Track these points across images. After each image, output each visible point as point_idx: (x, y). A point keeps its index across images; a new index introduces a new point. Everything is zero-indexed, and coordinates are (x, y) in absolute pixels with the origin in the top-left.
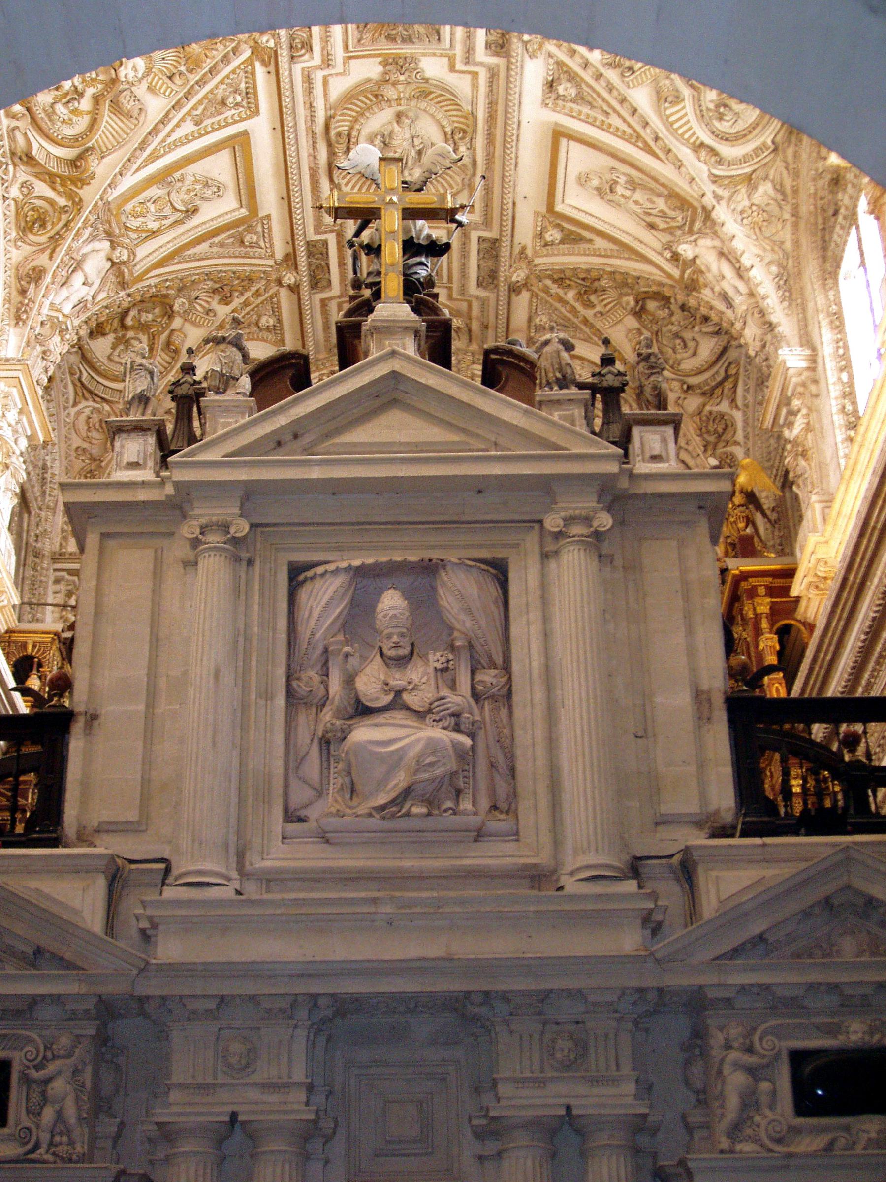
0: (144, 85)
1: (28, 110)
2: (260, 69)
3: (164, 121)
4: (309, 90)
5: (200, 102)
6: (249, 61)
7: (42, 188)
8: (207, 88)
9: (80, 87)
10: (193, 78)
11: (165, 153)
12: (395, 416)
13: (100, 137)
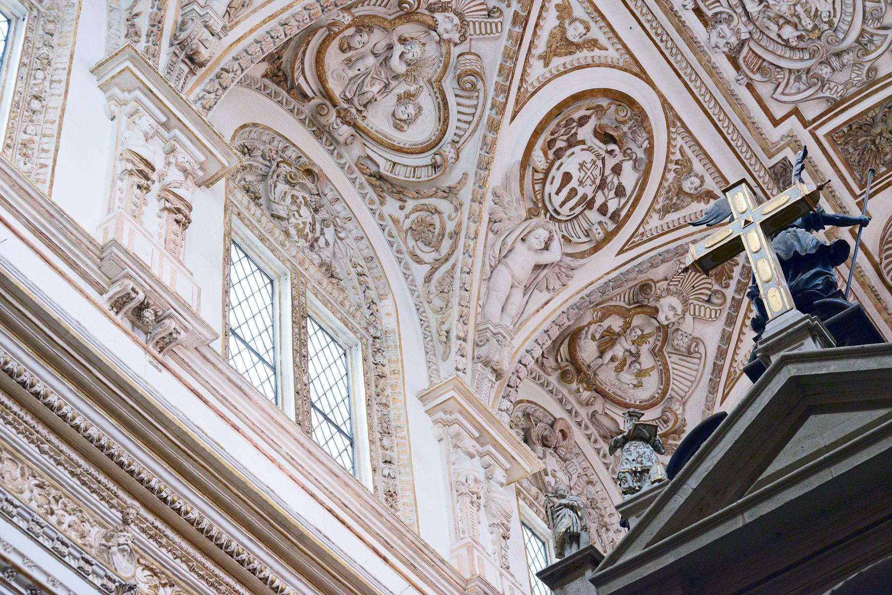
0: (689, 318)
9: (633, 350)
10: (730, 293)
12: (814, 422)
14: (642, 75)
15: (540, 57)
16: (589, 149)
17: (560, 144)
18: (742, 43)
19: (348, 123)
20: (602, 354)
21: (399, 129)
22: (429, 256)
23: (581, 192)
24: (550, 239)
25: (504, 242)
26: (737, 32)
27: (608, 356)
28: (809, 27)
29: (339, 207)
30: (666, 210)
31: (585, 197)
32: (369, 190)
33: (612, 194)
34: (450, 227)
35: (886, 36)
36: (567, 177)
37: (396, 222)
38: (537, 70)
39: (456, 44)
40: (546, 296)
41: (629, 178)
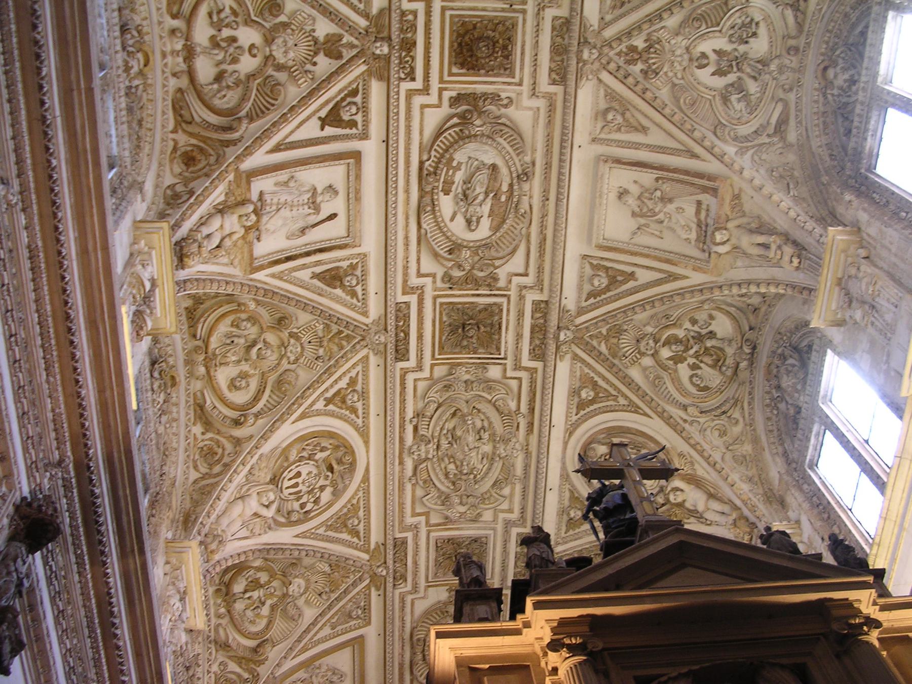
0: (303, 599)
1: (229, 611)
2: (374, 593)
3: (314, 624)
4: (403, 608)
5: (336, 614)
6: (368, 587)
7: (233, 666)
8: (341, 604)
11: (312, 647)
13: (273, 633)
14: (366, 442)
15: (325, 399)
16: (317, 467)
17: (305, 454)
18: (427, 459)
19: (207, 367)
20: (245, 591)
21: (230, 390)
22: (203, 469)
23: (300, 487)
24: (273, 502)
25: (248, 490)
26: (427, 452)
27: (247, 595)
28: (465, 471)
29: (175, 409)
30: (329, 528)
31: (300, 491)
32: (192, 412)
33: (312, 500)
34: (226, 460)
35: (497, 500)
36: (299, 474)
37: (195, 438)
38: (320, 405)
39: (289, 363)
40: (247, 534)
41: (326, 496)
